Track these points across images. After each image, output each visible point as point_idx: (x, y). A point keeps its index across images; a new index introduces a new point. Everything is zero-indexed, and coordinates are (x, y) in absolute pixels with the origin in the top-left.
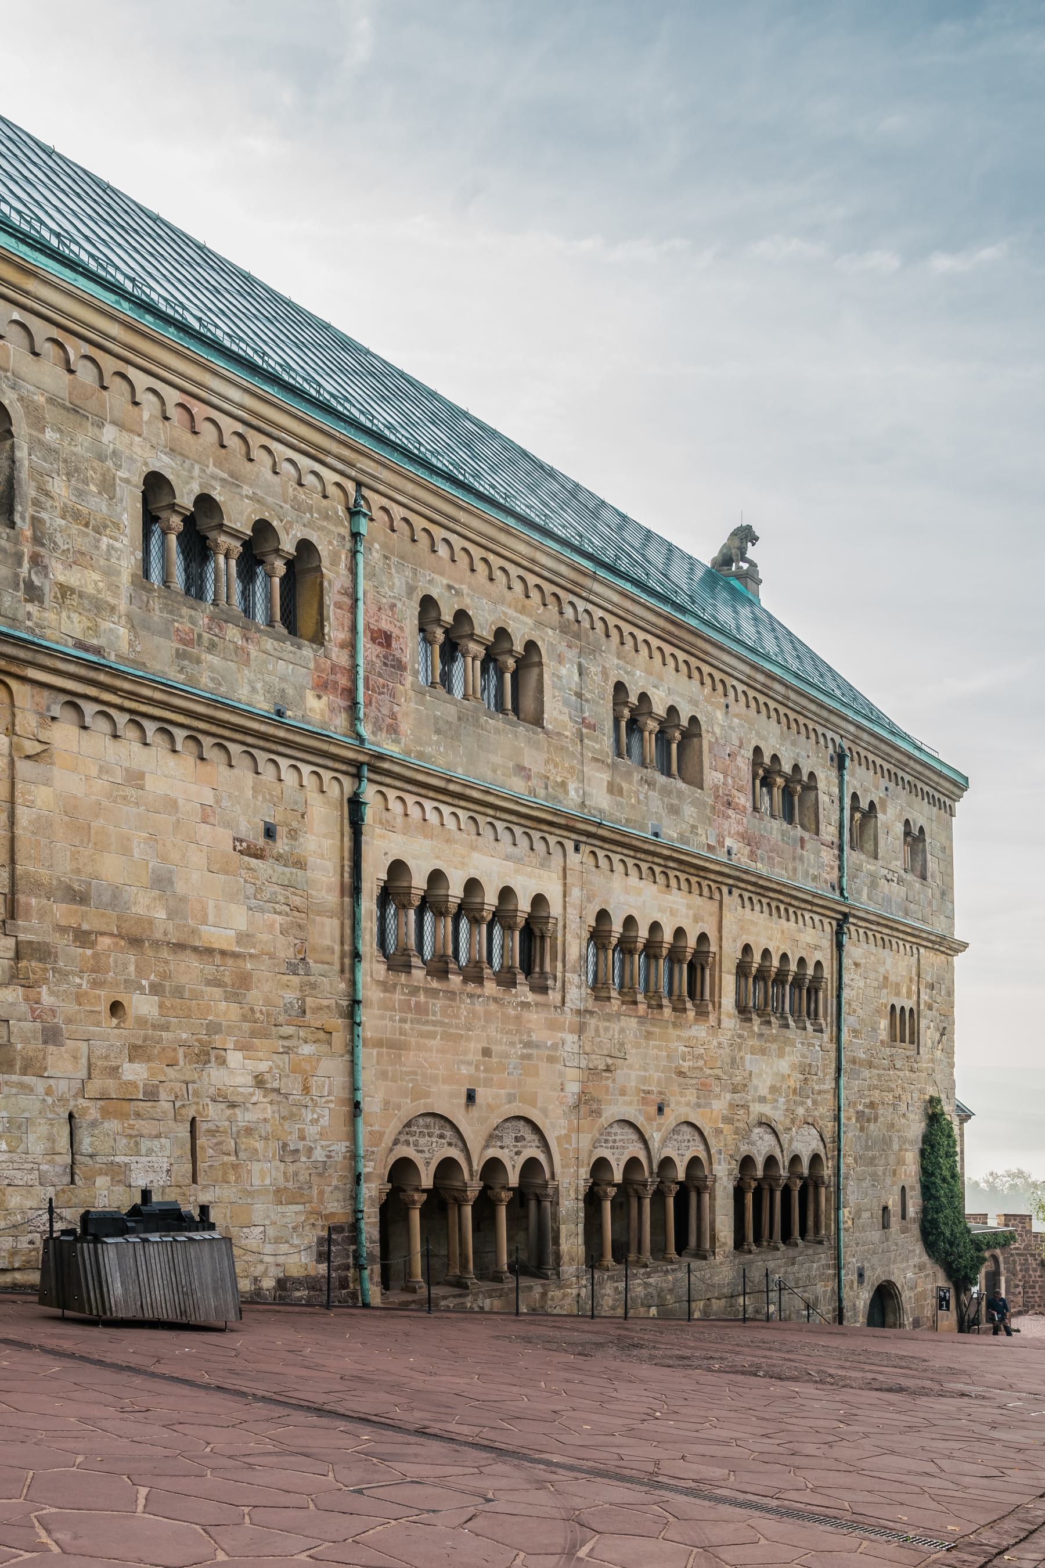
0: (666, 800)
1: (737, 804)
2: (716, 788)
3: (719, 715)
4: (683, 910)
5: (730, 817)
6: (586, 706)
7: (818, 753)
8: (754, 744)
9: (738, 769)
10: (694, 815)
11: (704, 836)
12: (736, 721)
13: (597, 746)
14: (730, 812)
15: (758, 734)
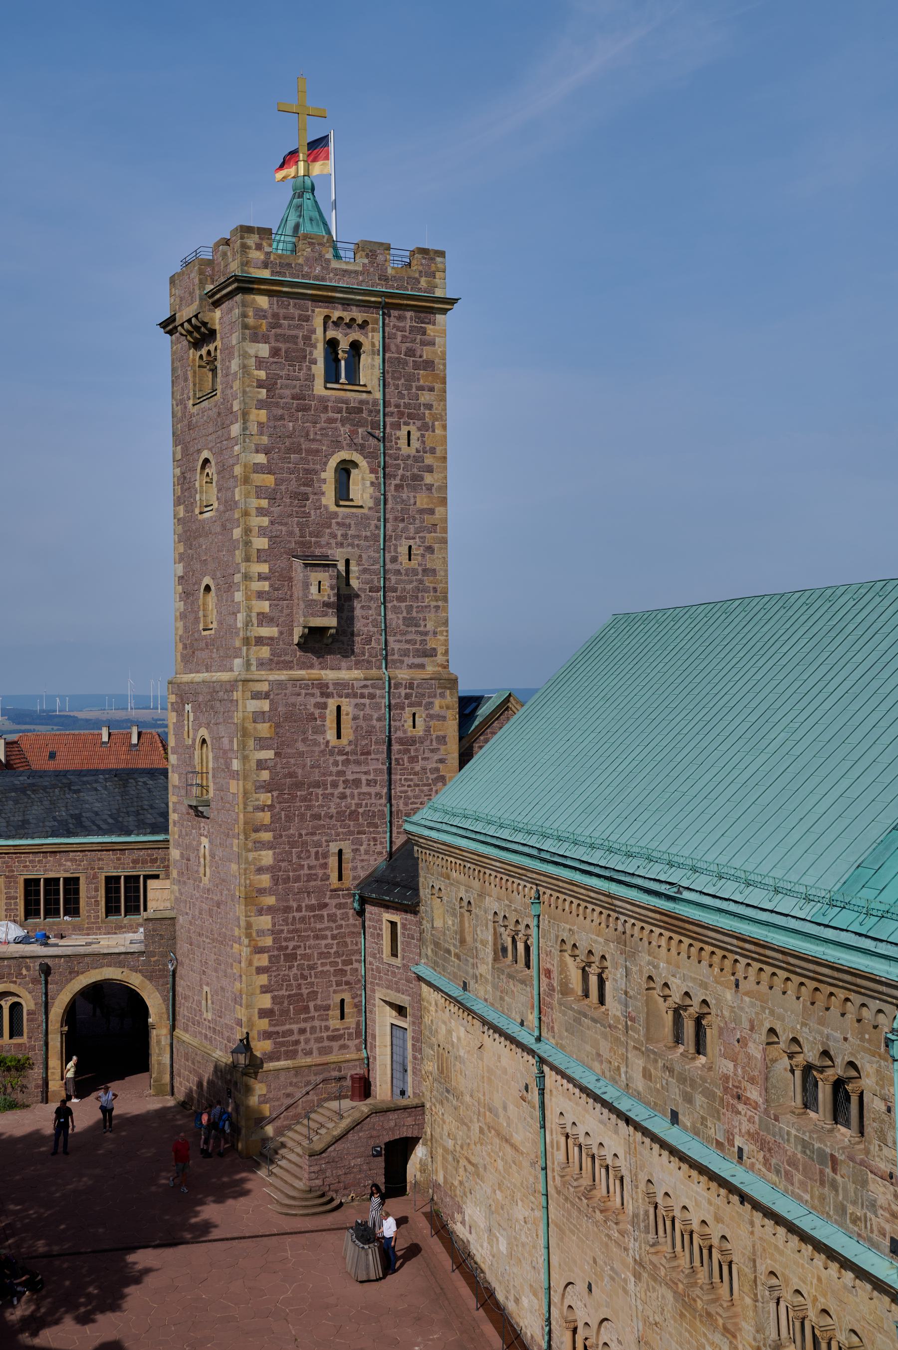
0: (681, 1086)
1: (748, 1098)
2: (726, 1078)
3: (729, 995)
4: (705, 1204)
5: (740, 1113)
6: (630, 1001)
7: (862, 1034)
8: (768, 1026)
9: (749, 1057)
10: (705, 1106)
11: (713, 1130)
12: (747, 999)
13: (636, 1036)
14: (741, 1107)
15: (772, 1013)
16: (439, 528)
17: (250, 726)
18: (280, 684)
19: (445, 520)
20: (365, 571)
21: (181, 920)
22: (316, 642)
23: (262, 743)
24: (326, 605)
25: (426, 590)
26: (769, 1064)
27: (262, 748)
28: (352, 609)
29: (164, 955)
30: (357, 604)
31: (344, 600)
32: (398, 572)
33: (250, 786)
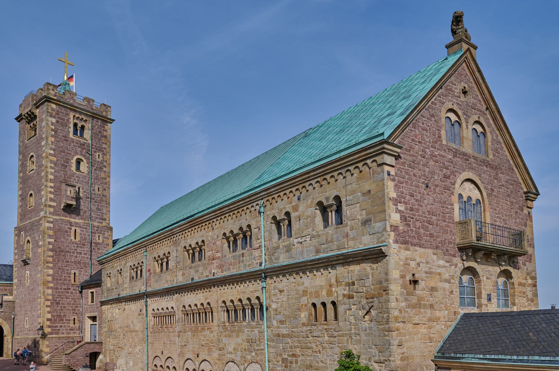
16: (108, 184)
17: (46, 231)
18: (56, 219)
19: (109, 182)
20: (84, 192)
21: (17, 301)
22: (68, 209)
23: (50, 237)
24: (72, 198)
25: (103, 201)
26: (222, 244)
27: (50, 238)
28: (80, 202)
29: (11, 313)
30: (81, 200)
31: (78, 199)
32: (95, 194)
33: (46, 249)
